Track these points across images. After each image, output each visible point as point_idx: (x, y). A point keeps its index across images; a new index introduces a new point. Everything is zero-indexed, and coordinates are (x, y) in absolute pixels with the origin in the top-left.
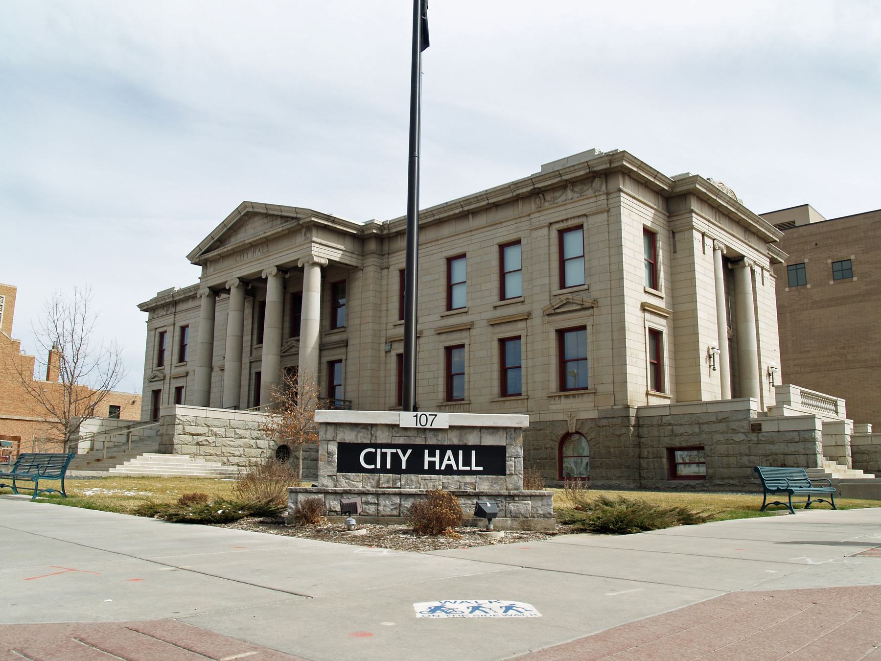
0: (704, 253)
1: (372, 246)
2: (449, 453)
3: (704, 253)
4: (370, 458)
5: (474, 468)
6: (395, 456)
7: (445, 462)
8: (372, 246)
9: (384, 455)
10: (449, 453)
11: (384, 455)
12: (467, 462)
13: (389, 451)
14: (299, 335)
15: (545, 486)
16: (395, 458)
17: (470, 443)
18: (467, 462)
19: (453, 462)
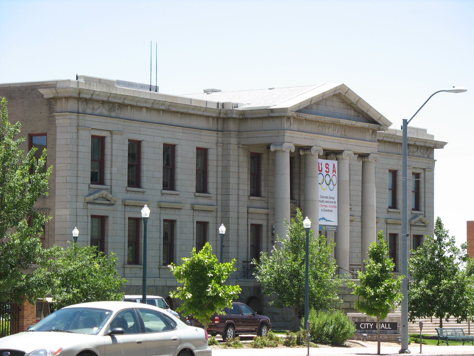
0: (274, 88)
1: (232, 126)
2: (383, 324)
3: (274, 88)
4: (363, 326)
5: (389, 328)
6: (369, 325)
7: (382, 327)
8: (232, 126)
9: (366, 325)
10: (383, 324)
11: (366, 325)
12: (387, 326)
13: (367, 324)
14: (148, 304)
15: (32, 324)
16: (369, 325)
17: (385, 322)
18: (387, 326)
19: (384, 327)
